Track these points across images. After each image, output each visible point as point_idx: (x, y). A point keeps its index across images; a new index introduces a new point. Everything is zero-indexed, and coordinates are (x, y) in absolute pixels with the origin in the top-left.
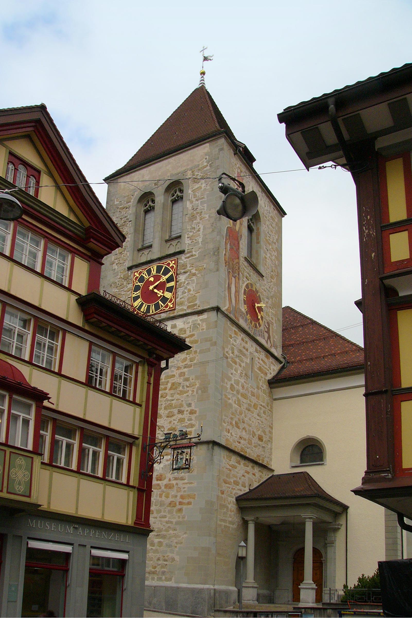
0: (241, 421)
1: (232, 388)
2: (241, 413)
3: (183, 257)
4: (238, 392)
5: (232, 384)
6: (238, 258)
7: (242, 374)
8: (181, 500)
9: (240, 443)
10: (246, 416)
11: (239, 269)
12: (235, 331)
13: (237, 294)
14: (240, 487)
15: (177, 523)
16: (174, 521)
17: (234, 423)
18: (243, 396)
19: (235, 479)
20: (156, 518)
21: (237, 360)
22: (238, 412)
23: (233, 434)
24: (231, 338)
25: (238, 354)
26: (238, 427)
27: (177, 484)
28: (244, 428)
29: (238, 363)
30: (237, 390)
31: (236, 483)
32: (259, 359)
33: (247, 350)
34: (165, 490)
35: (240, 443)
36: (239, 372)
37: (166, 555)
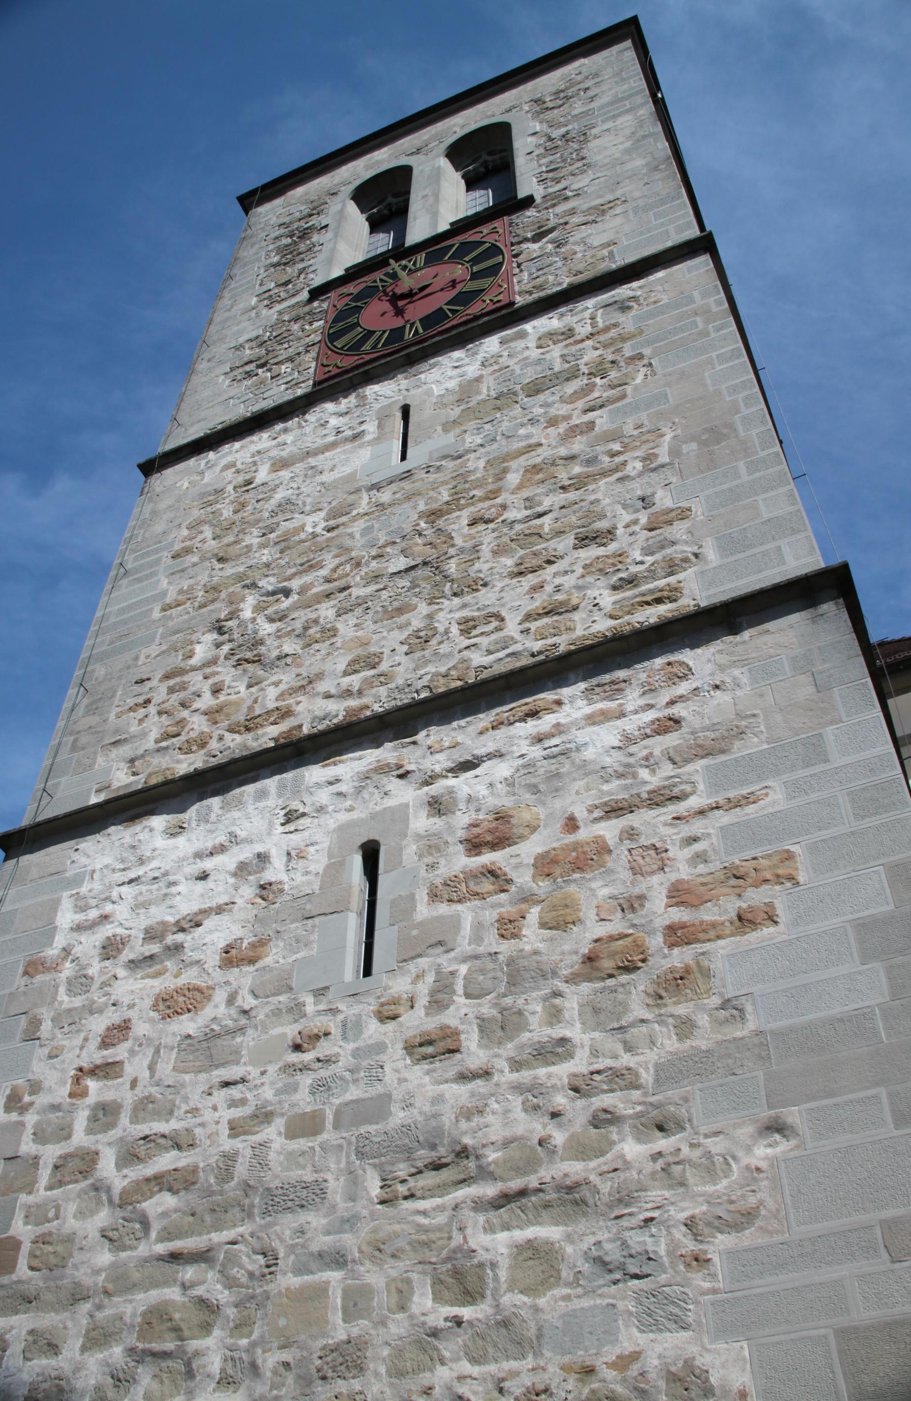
8: (678, 915)
15: (666, 1074)
16: (644, 1063)
20: (486, 1074)
27: (630, 834)
34: (543, 887)
37: (611, 1353)
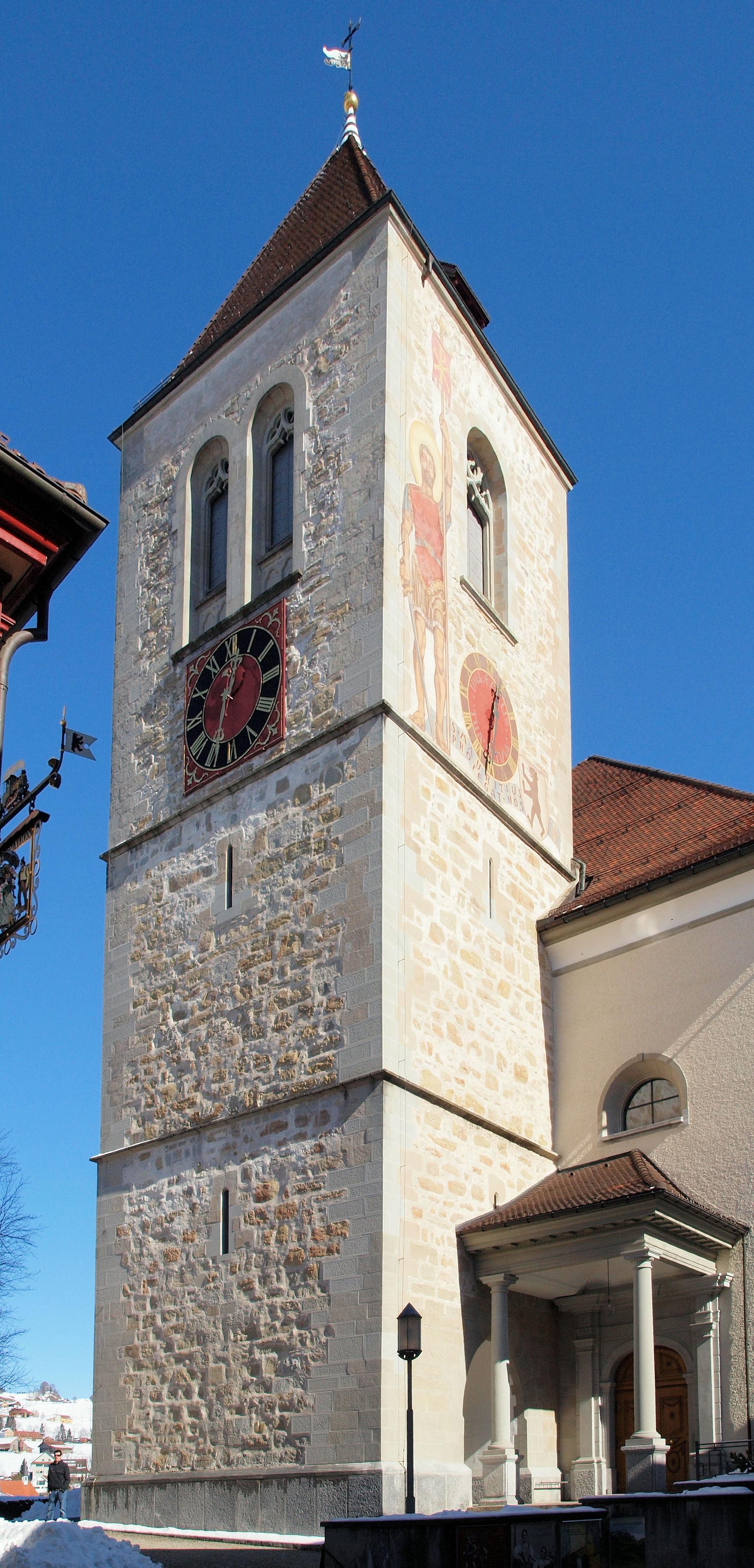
0: (465, 1026)
2: (463, 1003)
3: (298, 591)
4: (453, 946)
6: (442, 579)
7: (464, 898)
9: (463, 1082)
11: (445, 609)
12: (438, 780)
13: (441, 678)
14: (467, 1199)
19: (452, 1178)
21: (448, 859)
22: (455, 1000)
24: (429, 798)
25: (450, 844)
26: (457, 1041)
30: (450, 942)
31: (456, 1188)
36: (454, 892)
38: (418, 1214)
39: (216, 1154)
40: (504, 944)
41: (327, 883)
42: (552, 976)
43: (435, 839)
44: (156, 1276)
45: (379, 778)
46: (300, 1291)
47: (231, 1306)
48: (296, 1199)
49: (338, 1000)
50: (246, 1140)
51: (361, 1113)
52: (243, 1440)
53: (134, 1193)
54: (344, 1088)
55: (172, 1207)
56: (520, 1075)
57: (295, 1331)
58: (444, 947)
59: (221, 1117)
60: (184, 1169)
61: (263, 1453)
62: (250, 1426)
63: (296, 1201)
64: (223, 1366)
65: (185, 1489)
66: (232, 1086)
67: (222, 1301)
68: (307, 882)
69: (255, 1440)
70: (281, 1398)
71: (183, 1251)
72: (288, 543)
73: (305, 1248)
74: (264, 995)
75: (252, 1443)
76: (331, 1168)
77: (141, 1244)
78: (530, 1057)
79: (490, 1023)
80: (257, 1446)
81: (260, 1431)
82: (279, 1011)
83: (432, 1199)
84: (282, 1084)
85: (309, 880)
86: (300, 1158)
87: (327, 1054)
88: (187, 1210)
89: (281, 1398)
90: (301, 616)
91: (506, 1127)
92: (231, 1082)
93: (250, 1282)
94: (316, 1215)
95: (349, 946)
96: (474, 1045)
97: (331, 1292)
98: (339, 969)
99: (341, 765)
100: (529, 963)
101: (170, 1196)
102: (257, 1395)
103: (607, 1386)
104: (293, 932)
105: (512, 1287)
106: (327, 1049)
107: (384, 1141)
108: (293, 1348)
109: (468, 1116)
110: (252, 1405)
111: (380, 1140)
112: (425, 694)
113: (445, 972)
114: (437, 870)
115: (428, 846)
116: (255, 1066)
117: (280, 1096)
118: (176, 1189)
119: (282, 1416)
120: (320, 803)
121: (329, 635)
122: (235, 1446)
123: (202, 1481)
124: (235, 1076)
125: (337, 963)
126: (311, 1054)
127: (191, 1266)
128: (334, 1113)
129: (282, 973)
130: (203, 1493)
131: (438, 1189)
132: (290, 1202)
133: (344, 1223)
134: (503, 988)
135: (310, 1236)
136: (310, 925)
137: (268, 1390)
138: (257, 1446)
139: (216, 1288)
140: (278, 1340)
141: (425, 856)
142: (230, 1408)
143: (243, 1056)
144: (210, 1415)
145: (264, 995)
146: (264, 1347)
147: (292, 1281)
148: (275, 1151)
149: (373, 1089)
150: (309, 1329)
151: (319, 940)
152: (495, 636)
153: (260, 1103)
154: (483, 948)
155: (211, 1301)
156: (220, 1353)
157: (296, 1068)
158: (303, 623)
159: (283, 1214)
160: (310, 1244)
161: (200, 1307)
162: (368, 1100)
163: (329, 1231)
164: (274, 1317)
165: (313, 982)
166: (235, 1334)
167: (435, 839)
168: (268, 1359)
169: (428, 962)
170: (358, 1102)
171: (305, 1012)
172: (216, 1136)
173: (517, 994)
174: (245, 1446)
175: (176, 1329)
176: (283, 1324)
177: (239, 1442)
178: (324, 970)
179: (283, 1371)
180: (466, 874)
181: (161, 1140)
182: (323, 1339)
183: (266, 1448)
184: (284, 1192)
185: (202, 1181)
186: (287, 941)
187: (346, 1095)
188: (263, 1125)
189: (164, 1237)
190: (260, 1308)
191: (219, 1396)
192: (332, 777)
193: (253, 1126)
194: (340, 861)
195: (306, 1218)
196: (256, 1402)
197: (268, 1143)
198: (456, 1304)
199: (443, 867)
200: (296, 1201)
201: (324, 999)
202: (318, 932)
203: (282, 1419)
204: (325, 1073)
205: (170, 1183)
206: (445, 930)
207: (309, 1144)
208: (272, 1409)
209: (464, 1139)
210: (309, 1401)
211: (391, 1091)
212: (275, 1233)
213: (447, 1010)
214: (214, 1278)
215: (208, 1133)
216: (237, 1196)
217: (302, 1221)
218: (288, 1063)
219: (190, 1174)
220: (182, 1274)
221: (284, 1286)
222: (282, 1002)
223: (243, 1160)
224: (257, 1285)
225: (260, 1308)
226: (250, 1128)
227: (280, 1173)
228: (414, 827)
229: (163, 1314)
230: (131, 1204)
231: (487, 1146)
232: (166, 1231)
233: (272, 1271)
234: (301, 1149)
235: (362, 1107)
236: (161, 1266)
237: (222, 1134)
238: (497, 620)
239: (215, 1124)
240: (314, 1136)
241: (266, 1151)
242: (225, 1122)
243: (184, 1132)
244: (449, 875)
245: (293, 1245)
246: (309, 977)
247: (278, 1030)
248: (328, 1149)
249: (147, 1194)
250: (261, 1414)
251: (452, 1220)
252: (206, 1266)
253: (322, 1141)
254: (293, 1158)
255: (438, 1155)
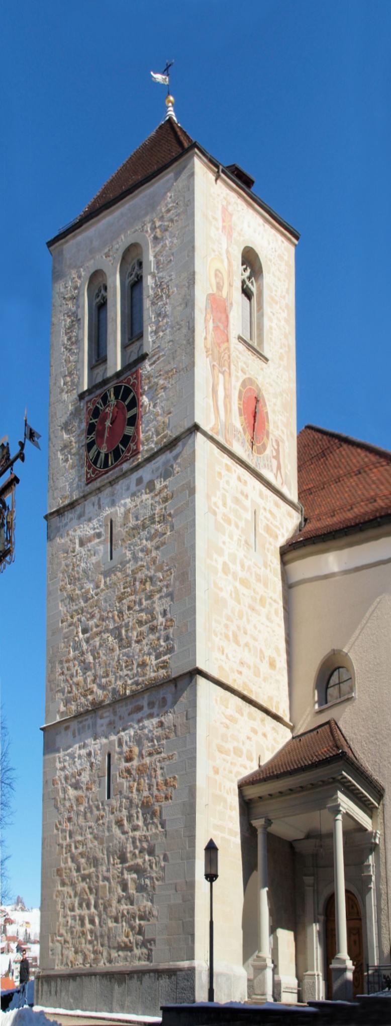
1: (226, 569)
2: (241, 616)
3: (147, 363)
4: (235, 575)
5: (225, 564)
9: (240, 673)
10: (248, 621)
12: (226, 465)
14: (243, 760)
17: (230, 634)
18: (244, 582)
19: (236, 744)
21: (232, 517)
23: (230, 656)
26: (237, 643)
28: (247, 645)
29: (233, 523)
30: (234, 573)
31: (238, 752)
32: (265, 509)
33: (247, 496)
35: (240, 673)
36: (235, 538)
38: (216, 772)
39: (104, 728)
40: (263, 569)
41: (165, 543)
42: (288, 587)
43: (225, 505)
44: (72, 815)
45: (193, 471)
46: (149, 826)
47: (111, 837)
48: (147, 760)
49: (171, 620)
50: (120, 718)
51: (184, 699)
52: (118, 943)
53: (62, 754)
54: (175, 681)
55: (81, 765)
56: (272, 665)
57: (147, 857)
58: (230, 577)
59: (107, 702)
60: (87, 738)
61: (129, 954)
62: (122, 932)
63: (148, 762)
64: (106, 883)
65: (86, 980)
66: (113, 680)
67: (107, 834)
68: (154, 543)
69: (125, 943)
70: (139, 910)
71: (86, 796)
72: (141, 336)
73: (152, 795)
74: (130, 619)
75: (123, 945)
76: (167, 738)
77: (65, 791)
78: (277, 649)
79: (255, 628)
80: (127, 948)
81: (127, 936)
82: (139, 629)
83: (224, 760)
84: (141, 679)
85: (155, 541)
86: (150, 731)
87: (166, 658)
88: (88, 768)
89: (139, 910)
90: (149, 378)
91: (265, 704)
92: (112, 678)
93: (122, 820)
94: (159, 772)
95: (177, 583)
96: (247, 645)
97: (167, 828)
98: (172, 600)
99: (172, 466)
100: (276, 579)
101: (80, 757)
102: (125, 907)
103: (322, 918)
104: (146, 576)
105: (270, 829)
106: (165, 654)
107: (198, 718)
108: (145, 870)
109: (244, 698)
110: (123, 915)
111: (195, 718)
112: (218, 413)
113: (231, 595)
114: (226, 525)
115: (221, 510)
116: (126, 667)
117: (139, 687)
118: (83, 752)
119: (140, 925)
120: (160, 492)
121: (164, 388)
122: (114, 948)
123: (95, 974)
124: (115, 674)
125: (170, 595)
126: (157, 658)
127: (90, 807)
128: (169, 698)
129: (140, 603)
130: (96, 983)
131: (227, 752)
132: (144, 762)
133: (174, 778)
134: (262, 601)
135: (155, 787)
136: (156, 571)
137: (132, 904)
138: (127, 948)
139: (103, 824)
140: (138, 865)
141: (219, 517)
142: (111, 917)
143: (119, 660)
144: (100, 922)
145: (130, 619)
146: (130, 869)
147: (145, 820)
148: (136, 726)
149: (191, 681)
150: (154, 856)
151: (161, 581)
152: (258, 362)
153: (128, 692)
154: (251, 574)
155: (100, 834)
156: (106, 874)
157: (148, 668)
158: (150, 383)
159: (141, 770)
160: (156, 792)
161: (95, 838)
162: (188, 689)
163: (166, 783)
164: (135, 847)
165: (158, 609)
166: (114, 859)
167: (225, 505)
168: (132, 879)
169: (221, 589)
170: (183, 691)
171: (153, 629)
172: (105, 715)
173: (270, 604)
174: (119, 948)
175: (82, 855)
176: (140, 852)
177: (116, 945)
178: (164, 601)
179: (141, 888)
180: (242, 524)
181: (75, 717)
182: (163, 864)
183: (131, 950)
184: (141, 755)
185: (95, 745)
186: (143, 582)
187: (176, 686)
188: (130, 707)
189: (76, 786)
190: (127, 839)
191: (105, 908)
192: (167, 474)
193: (124, 708)
194: (172, 527)
195: (153, 773)
196: (125, 912)
197: (132, 720)
198: (238, 840)
199: (229, 523)
200: (148, 762)
201: (164, 620)
202: (160, 575)
203: (140, 926)
204: (164, 671)
205: (80, 748)
206: (231, 565)
207: (155, 721)
208: (134, 918)
209: (242, 715)
210: (155, 913)
211: (201, 682)
212: (136, 784)
213: (232, 621)
214: (102, 817)
215: (100, 713)
216: (115, 757)
217: (151, 776)
218: (143, 665)
219: (90, 741)
220: (85, 813)
221: (140, 823)
222: (140, 623)
223: (118, 733)
224: (125, 822)
225: (127, 839)
226: (123, 710)
227: (139, 741)
228: (214, 499)
229: (75, 842)
230: (60, 762)
231: (254, 720)
232: (78, 782)
233: (134, 812)
234: (151, 724)
235: (185, 695)
236: (75, 808)
237: (107, 714)
238: (258, 352)
239: (104, 707)
240: (158, 715)
241: (131, 726)
242: (109, 705)
243: (87, 712)
244: (233, 527)
245: (146, 793)
246: (155, 605)
247: (138, 642)
248: (166, 724)
249: (68, 755)
250: (128, 922)
251: (236, 777)
252: (98, 808)
253: (162, 719)
254: (146, 731)
255: (227, 727)
